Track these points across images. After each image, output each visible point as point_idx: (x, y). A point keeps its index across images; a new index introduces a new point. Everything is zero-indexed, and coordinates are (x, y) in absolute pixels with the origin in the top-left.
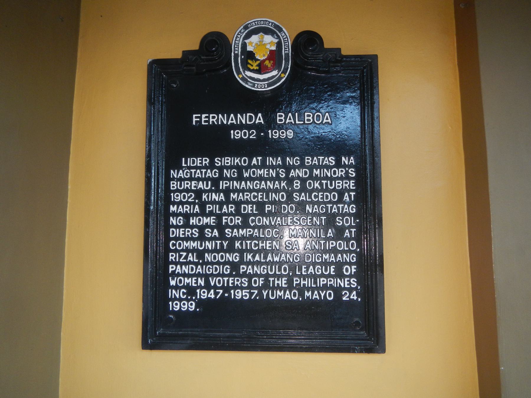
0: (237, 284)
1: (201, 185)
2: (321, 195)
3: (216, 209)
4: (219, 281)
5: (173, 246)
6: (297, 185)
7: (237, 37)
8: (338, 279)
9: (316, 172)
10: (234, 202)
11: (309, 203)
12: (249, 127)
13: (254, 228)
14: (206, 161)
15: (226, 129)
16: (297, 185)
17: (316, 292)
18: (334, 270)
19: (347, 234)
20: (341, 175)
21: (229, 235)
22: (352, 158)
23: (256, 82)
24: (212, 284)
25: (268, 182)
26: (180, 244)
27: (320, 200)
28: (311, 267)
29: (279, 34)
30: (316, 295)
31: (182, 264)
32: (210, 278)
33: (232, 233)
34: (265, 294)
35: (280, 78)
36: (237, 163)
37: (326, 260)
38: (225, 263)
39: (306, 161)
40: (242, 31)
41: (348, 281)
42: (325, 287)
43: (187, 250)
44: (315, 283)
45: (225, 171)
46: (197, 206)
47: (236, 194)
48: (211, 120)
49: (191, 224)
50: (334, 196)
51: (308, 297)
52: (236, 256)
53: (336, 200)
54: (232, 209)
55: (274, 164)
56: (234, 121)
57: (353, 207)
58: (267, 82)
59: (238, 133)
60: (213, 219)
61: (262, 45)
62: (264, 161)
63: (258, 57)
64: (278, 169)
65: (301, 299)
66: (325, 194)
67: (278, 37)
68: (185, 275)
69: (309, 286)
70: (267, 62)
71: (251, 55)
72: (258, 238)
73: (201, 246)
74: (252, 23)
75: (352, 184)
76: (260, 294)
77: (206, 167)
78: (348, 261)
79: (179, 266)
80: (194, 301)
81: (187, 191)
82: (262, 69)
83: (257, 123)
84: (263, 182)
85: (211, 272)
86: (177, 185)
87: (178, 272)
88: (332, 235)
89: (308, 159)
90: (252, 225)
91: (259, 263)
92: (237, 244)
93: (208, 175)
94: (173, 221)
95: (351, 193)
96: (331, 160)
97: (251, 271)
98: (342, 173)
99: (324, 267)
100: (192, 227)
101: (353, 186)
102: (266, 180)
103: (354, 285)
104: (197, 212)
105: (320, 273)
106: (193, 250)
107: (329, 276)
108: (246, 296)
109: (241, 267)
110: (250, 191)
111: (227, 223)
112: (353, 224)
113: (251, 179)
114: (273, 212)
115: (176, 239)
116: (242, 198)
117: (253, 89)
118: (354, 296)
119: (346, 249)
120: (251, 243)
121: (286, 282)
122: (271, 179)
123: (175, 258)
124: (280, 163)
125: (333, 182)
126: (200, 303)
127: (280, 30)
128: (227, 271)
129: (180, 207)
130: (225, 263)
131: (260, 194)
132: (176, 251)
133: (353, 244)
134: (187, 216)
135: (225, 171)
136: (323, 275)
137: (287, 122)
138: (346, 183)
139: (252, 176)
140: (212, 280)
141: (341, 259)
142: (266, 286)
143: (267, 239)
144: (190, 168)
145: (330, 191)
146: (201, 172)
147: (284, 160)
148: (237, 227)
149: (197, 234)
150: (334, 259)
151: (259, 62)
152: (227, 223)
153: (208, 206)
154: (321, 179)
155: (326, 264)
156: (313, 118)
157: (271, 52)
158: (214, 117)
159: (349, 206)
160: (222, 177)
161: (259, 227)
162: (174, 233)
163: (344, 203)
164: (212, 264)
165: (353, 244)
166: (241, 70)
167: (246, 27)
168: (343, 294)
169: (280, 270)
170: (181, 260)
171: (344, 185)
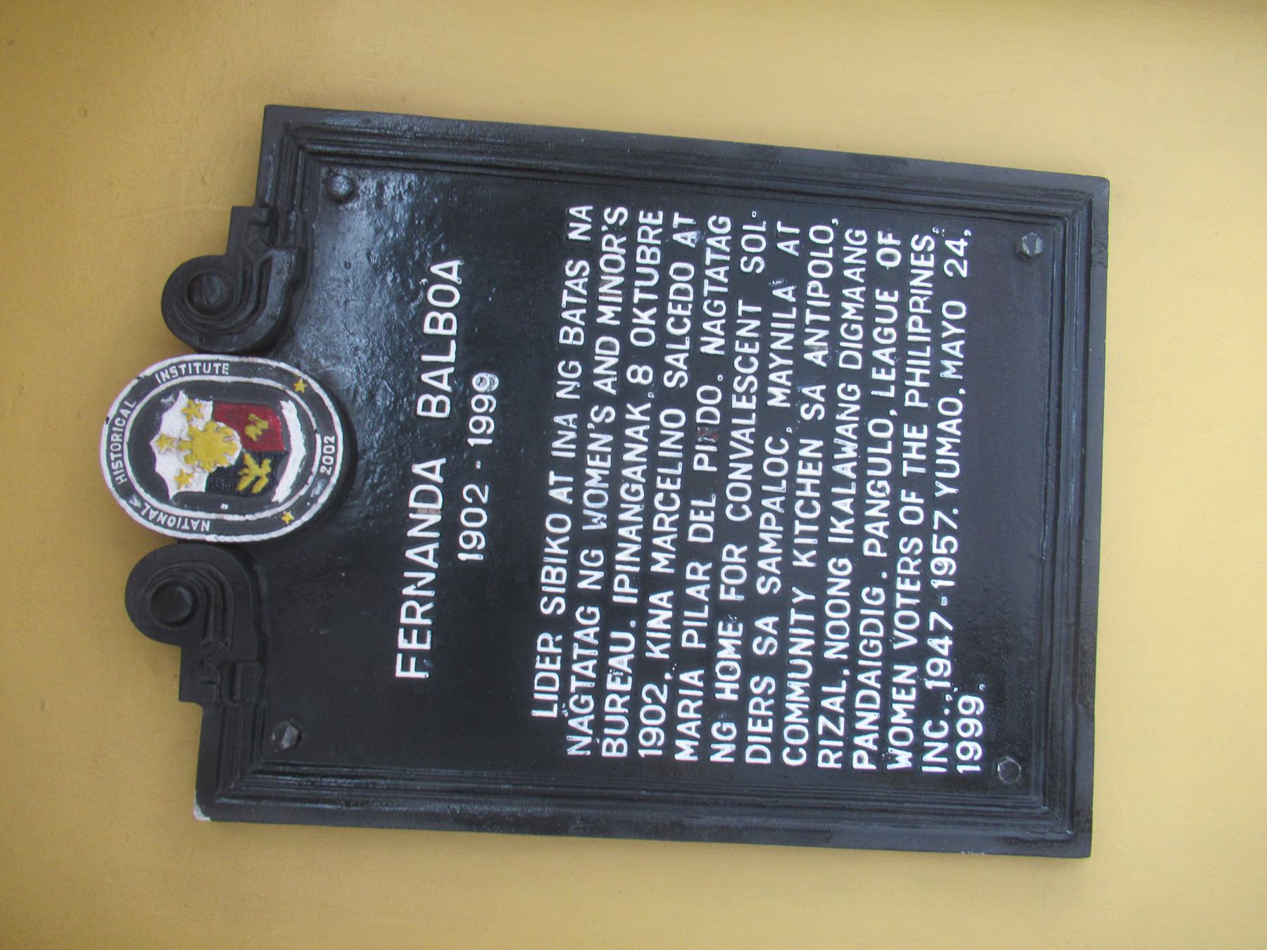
0: (916, 568)
1: (621, 662)
2: (675, 307)
3: (695, 619)
4: (905, 620)
6: (640, 374)
7: (155, 521)
8: (912, 283)
9: (607, 315)
10: (678, 564)
11: (696, 344)
12: (453, 504)
13: (758, 509)
14: (547, 643)
15: (452, 574)
16: (640, 374)
17: (945, 347)
18: (886, 293)
19: (789, 247)
20: (620, 245)
21: (774, 585)
22: (573, 211)
23: (315, 470)
24: (912, 641)
26: (796, 734)
28: (877, 354)
29: (163, 387)
30: (953, 348)
31: (852, 732)
33: (768, 574)
34: (946, 490)
35: (310, 397)
36: (561, 546)
37: (859, 312)
38: (856, 602)
40: (137, 503)
41: (917, 258)
42: (933, 321)
43: (813, 712)
44: (920, 346)
45: (583, 585)
46: (684, 677)
48: (418, 620)
49: (735, 697)
50: (680, 272)
51: (959, 370)
53: (691, 268)
54: (697, 571)
55: (572, 435)
56: (431, 548)
57: (715, 224)
58: (318, 437)
59: (468, 540)
60: (725, 628)
61: (191, 446)
62: (563, 466)
63: (232, 460)
64: (590, 426)
66: (672, 297)
67: (173, 391)
68: (884, 723)
69: (927, 363)
71: (224, 484)
73: (802, 669)
74: (111, 471)
76: (945, 504)
77: (567, 645)
79: (858, 740)
80: (956, 697)
81: (634, 704)
82: (271, 450)
84: (627, 472)
85: (878, 643)
86: (615, 737)
87: (875, 742)
88: (791, 289)
89: (566, 336)
90: (749, 514)
91: (860, 503)
92: (804, 561)
94: (722, 754)
96: (576, 269)
97: (882, 525)
98: (616, 242)
99: (878, 320)
100: (745, 693)
101: (655, 217)
102: (619, 464)
104: (700, 678)
105: (892, 331)
106: (815, 693)
107: (902, 306)
108: (949, 545)
109: (867, 553)
110: (648, 512)
111: (740, 590)
112: (763, 229)
113: (614, 508)
114: (713, 449)
115: (777, 744)
116: (669, 538)
117: (334, 480)
118: (959, 246)
119: (830, 255)
120: (803, 521)
121: (914, 429)
122: (618, 448)
123: (834, 749)
126: (963, 681)
127: (151, 382)
128: (877, 597)
129: (681, 728)
130: (856, 602)
132: (813, 747)
133: (817, 234)
134: (712, 709)
135: (583, 585)
136: (900, 326)
137: (448, 389)
138: (645, 234)
139: (604, 504)
140: (902, 640)
141: (858, 270)
142: (923, 485)
143: (792, 476)
144: (564, 694)
145: (665, 282)
146: (582, 658)
147: (566, 406)
148: (752, 557)
149: (767, 679)
150: (858, 290)
152: (740, 590)
154: (627, 304)
155: (870, 313)
156: (442, 310)
157: (216, 416)
158: (411, 612)
159: (713, 235)
160: (602, 597)
161: (758, 495)
162: (758, 753)
163: (701, 246)
164: (855, 638)
165: (819, 234)
167: (126, 491)
169: (881, 443)
170: (841, 733)
171: (650, 240)
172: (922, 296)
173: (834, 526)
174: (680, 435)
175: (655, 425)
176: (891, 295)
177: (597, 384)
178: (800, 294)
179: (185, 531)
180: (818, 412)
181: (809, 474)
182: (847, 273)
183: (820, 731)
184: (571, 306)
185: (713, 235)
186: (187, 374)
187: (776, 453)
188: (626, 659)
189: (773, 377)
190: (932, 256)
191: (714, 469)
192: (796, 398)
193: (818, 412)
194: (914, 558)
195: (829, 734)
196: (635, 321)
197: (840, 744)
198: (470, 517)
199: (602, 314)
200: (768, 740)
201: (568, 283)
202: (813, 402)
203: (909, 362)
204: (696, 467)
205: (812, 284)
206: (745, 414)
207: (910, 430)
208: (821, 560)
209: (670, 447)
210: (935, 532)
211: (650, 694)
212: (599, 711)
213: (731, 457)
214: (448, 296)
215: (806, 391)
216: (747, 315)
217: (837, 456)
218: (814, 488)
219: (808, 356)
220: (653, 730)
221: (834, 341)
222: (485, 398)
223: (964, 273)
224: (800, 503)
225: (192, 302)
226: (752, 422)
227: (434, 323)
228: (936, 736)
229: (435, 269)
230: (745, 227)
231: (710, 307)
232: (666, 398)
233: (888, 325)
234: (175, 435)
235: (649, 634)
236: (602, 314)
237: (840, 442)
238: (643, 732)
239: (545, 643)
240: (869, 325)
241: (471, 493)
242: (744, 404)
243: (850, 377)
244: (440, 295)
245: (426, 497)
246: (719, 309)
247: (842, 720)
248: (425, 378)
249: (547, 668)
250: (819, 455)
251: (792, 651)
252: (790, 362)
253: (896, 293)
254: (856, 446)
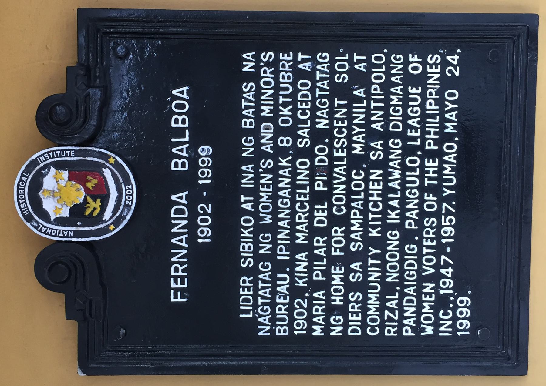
0: (433, 234)
1: (283, 289)
2: (301, 105)
4: (428, 260)
5: (375, 331)
6: (285, 141)
7: (45, 233)
8: (428, 82)
9: (266, 111)
10: (309, 238)
11: (314, 123)
14: (245, 281)
16: (285, 141)
17: (447, 116)
18: (414, 88)
19: (361, 67)
20: (271, 73)
21: (359, 246)
22: (244, 56)
23: (123, 203)
24: (432, 270)
25: (280, 185)
27: (309, 107)
28: (410, 122)
29: (42, 165)
31: (402, 317)
32: (424, 274)
33: (356, 241)
34: (448, 192)
35: (117, 165)
36: (249, 233)
38: (403, 253)
39: (248, 126)
40: (35, 224)
41: (431, 68)
43: (381, 309)
44: (433, 116)
45: (261, 251)
46: (315, 295)
47: (297, 234)
48: (180, 273)
49: (342, 303)
50: (303, 85)
51: (455, 128)
52: (391, 235)
53: (309, 83)
55: (252, 176)
56: (184, 237)
57: (321, 57)
58: (123, 186)
59: (202, 232)
60: (335, 269)
61: (59, 193)
62: (247, 192)
64: (261, 170)
65: (456, 139)
66: (299, 99)
67: (47, 166)
68: (418, 313)
69: (437, 125)
70: (90, 185)
71: (77, 212)
72: (366, 202)
73: (375, 288)
74: (21, 209)
75: (286, 57)
76: (448, 199)
77: (255, 282)
78: (402, 66)
79: (405, 322)
80: (456, 298)
81: (291, 309)
83: (186, 203)
84: (281, 193)
85: (414, 272)
86: (282, 326)
87: (414, 322)
88: (362, 90)
89: (245, 123)
90: (345, 210)
91: (403, 201)
92: (374, 233)
93: (267, 278)
94: (336, 331)
95: (299, 60)
96: (248, 87)
97: (414, 212)
98: (268, 71)
99: (410, 103)
100: (346, 301)
101: (289, 56)
102: (277, 189)
103: (437, 59)
104: (323, 295)
105: (418, 109)
106: (382, 299)
107: (423, 95)
108: (451, 221)
109: (407, 227)
110: (293, 213)
112: (347, 58)
113: (275, 212)
114: (325, 178)
115: (364, 325)
116: (304, 226)
117: (133, 208)
118: (453, 59)
119: (383, 70)
120: (374, 213)
121: (431, 161)
122: (276, 181)
123: (393, 327)
124: (250, 166)
125: (281, 85)
126: (459, 290)
127: (35, 163)
129: (315, 320)
130: (403, 253)
131: (298, 199)
132: (382, 326)
134: (330, 310)
135: (261, 251)
136: (422, 106)
137: (187, 155)
138: (284, 66)
139: (270, 210)
141: (399, 77)
142: (436, 190)
144: (255, 306)
145: (296, 91)
146: (263, 288)
147: (247, 161)
148: (347, 233)
149: (358, 294)
150: (399, 88)
151: (88, 198)
152: (341, 250)
153: (315, 278)
154: (276, 104)
155: (405, 100)
156: (180, 114)
157: (70, 179)
158: (176, 270)
159: (320, 63)
160: (272, 257)
161: (350, 201)
162: (354, 329)
164: (402, 271)
165: (377, 59)
166: (101, 226)
167: (29, 219)
168: (449, 75)
169: (413, 169)
170: (396, 318)
171: (287, 69)
172: (433, 88)
173: (390, 215)
174: (307, 172)
175: (294, 168)
176: (417, 89)
177: (263, 148)
178: (368, 93)
179: (61, 237)
180: (379, 155)
181: (376, 188)
182: (393, 79)
183: (386, 318)
184: (247, 107)
185: (320, 63)
186: (54, 157)
187: (357, 178)
188: (285, 287)
189: (355, 138)
190: (439, 66)
191: (326, 189)
192: (367, 149)
193: (379, 155)
194: (432, 228)
195: (390, 319)
196: (281, 113)
197: (396, 324)
198: (202, 221)
199: (264, 111)
200: (359, 324)
201: (245, 95)
202: (376, 150)
203: (428, 125)
204: (316, 188)
205: (374, 86)
206: (341, 159)
207: (428, 162)
208: (383, 232)
209: (302, 178)
210: (443, 214)
211: (299, 304)
212: (273, 313)
213: (335, 182)
214: (183, 106)
215: (372, 144)
216: (340, 106)
217: (390, 178)
218: (378, 195)
219: (373, 126)
220: (301, 322)
221: (386, 117)
222: (206, 159)
223: (457, 74)
224: (372, 203)
225: (52, 119)
226: (345, 163)
227: (176, 121)
228: (446, 318)
229: (174, 92)
230: (337, 58)
231: (320, 103)
232: (299, 153)
233: (416, 106)
234: (51, 189)
235: (296, 274)
236: (264, 111)
237: (392, 170)
238: (296, 322)
239: (244, 281)
240: (405, 107)
241: (202, 208)
242: (340, 154)
243: (396, 135)
244: (178, 106)
246: (325, 103)
247: (397, 312)
248: (174, 150)
249: (246, 294)
250: (381, 178)
251: (370, 279)
252: (364, 130)
253: (420, 88)
254: (400, 172)
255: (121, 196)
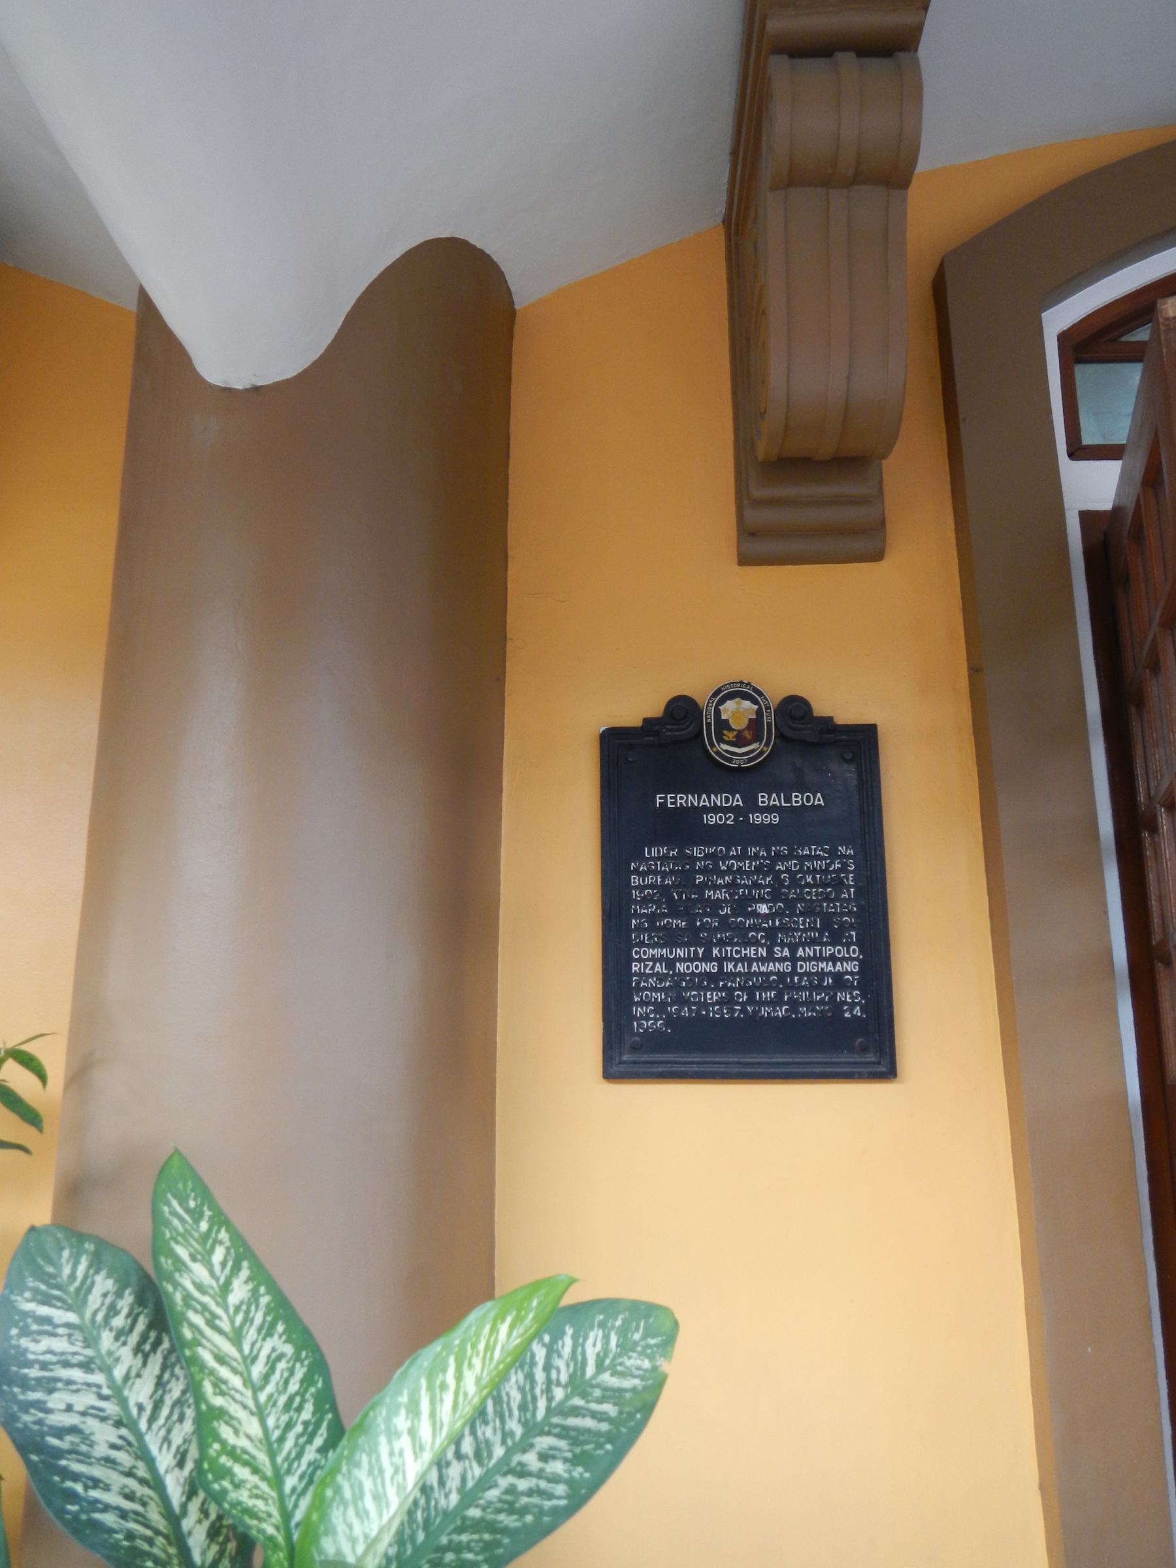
12: (725, 810)
26: (645, 953)
43: (653, 959)
61: (737, 712)
62: (744, 850)
71: (723, 725)
73: (671, 953)
76: (744, 1011)
82: (740, 741)
92: (715, 951)
106: (661, 959)
126: (669, 1021)
132: (640, 960)
142: (751, 1000)
157: (750, 720)
158: (681, 798)
184: (810, 849)
208: (716, 959)
214: (808, 801)
245: (727, 799)
255: (740, 755)
